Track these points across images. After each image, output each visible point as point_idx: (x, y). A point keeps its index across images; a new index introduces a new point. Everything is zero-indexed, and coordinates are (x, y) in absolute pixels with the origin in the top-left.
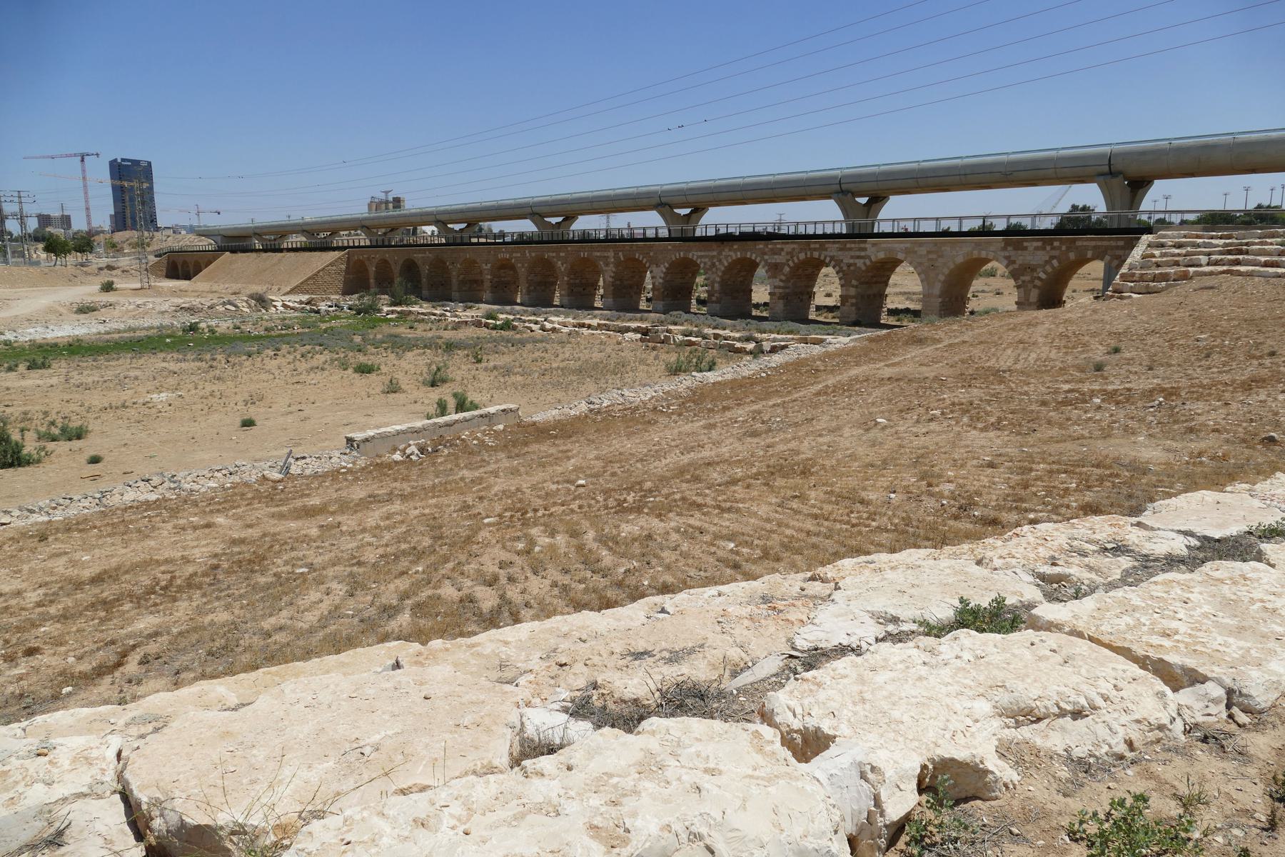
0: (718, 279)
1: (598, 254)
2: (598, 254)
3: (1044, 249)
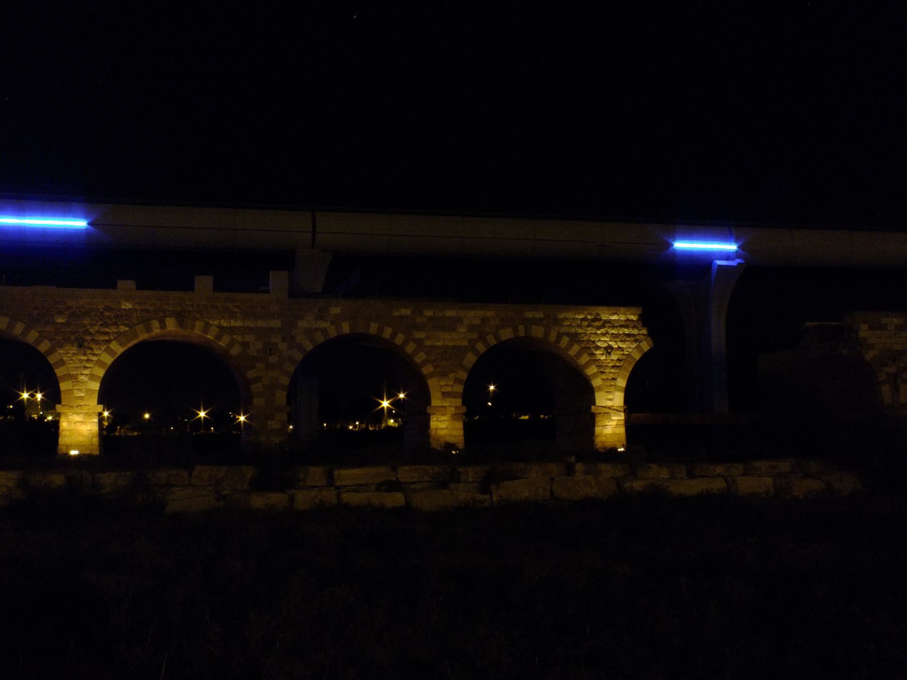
0: (285, 381)
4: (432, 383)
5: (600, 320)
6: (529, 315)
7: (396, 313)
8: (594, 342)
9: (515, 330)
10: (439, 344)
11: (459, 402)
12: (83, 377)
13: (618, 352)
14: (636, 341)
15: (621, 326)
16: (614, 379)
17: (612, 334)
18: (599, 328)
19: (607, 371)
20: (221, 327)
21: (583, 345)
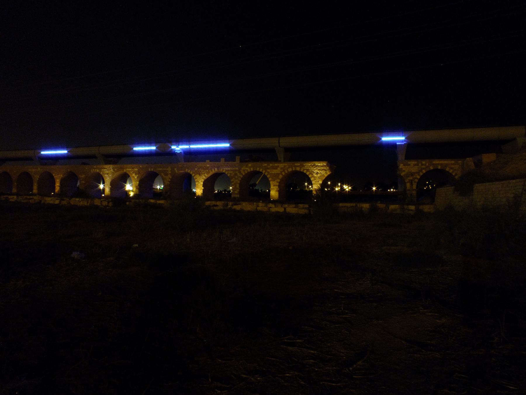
0: (239, 182)
1: (161, 169)
2: (161, 169)
3: (418, 165)
4: (271, 183)
5: (315, 165)
6: (296, 164)
7: (263, 165)
8: (313, 171)
9: (292, 169)
10: (273, 173)
11: (277, 187)
12: (200, 181)
13: (320, 174)
14: (325, 171)
15: (321, 167)
16: (318, 181)
18: (315, 167)
19: (316, 179)
20: (226, 170)
21: (310, 172)
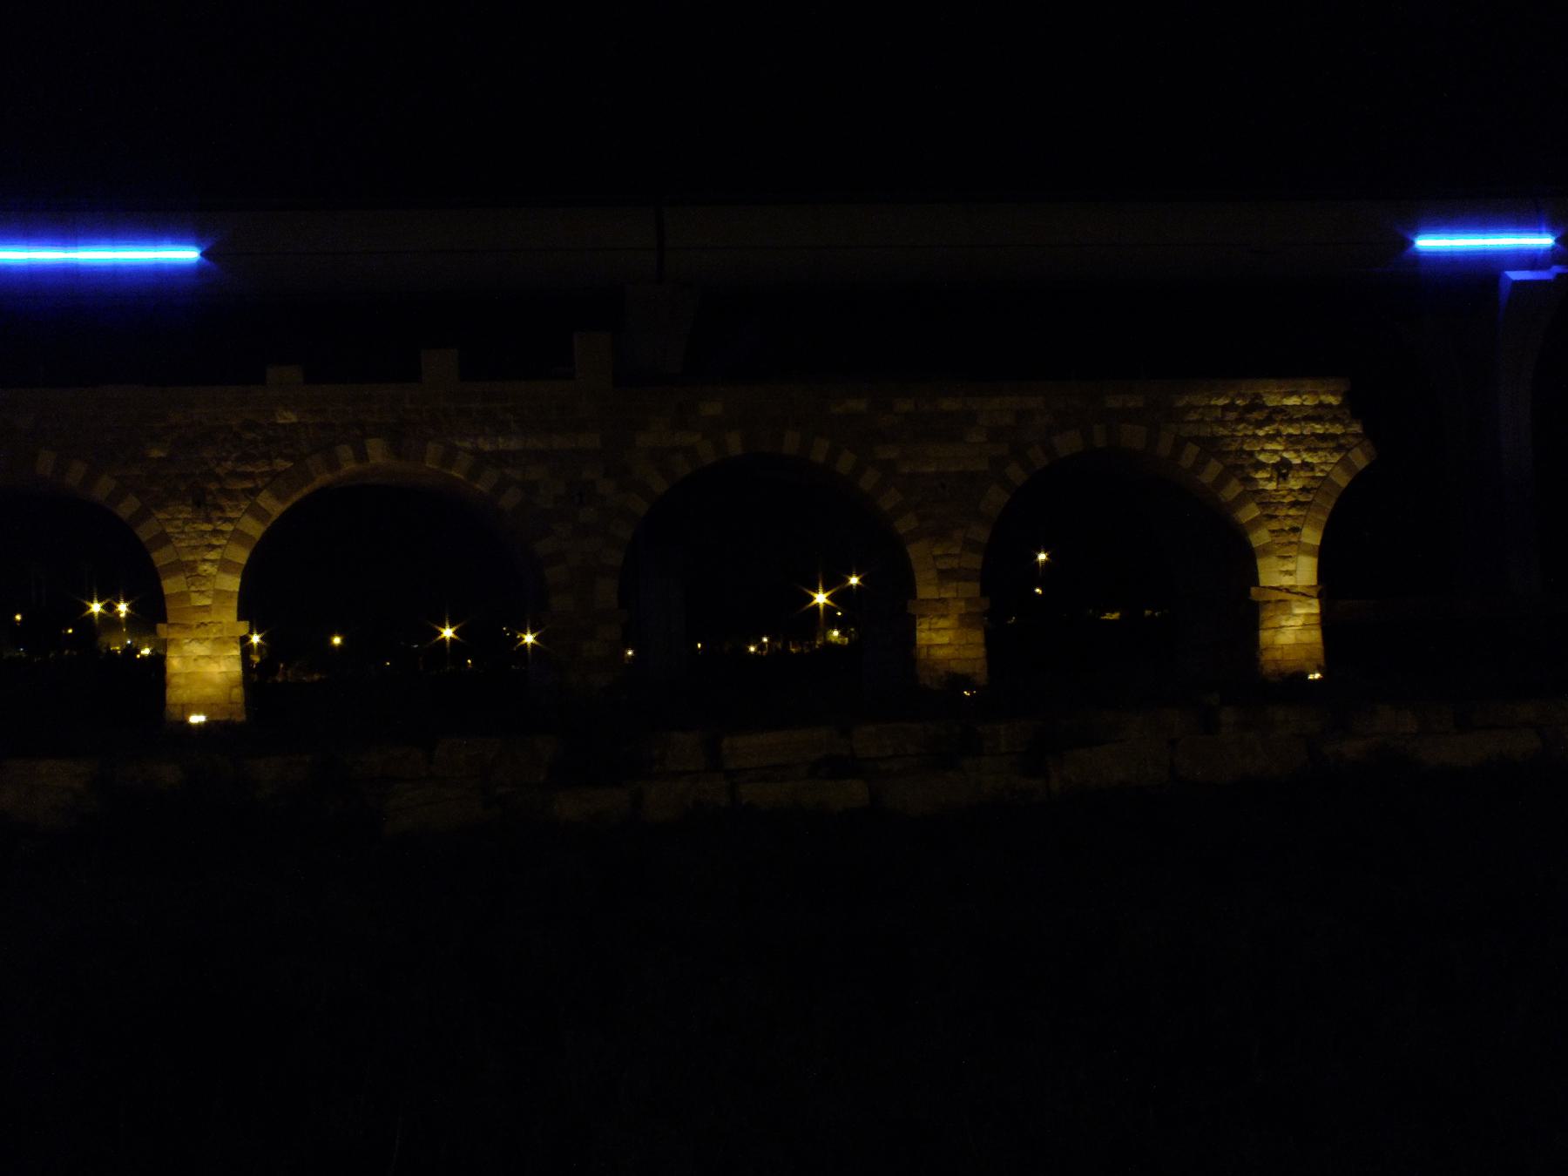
4: (916, 552)
5: (1263, 407)
8: (1251, 454)
10: (931, 469)
11: (973, 588)
12: (206, 567)
13: (1302, 473)
14: (1339, 448)
15: (1308, 419)
16: (1295, 530)
17: (1290, 436)
18: (1260, 425)
19: (1281, 513)
